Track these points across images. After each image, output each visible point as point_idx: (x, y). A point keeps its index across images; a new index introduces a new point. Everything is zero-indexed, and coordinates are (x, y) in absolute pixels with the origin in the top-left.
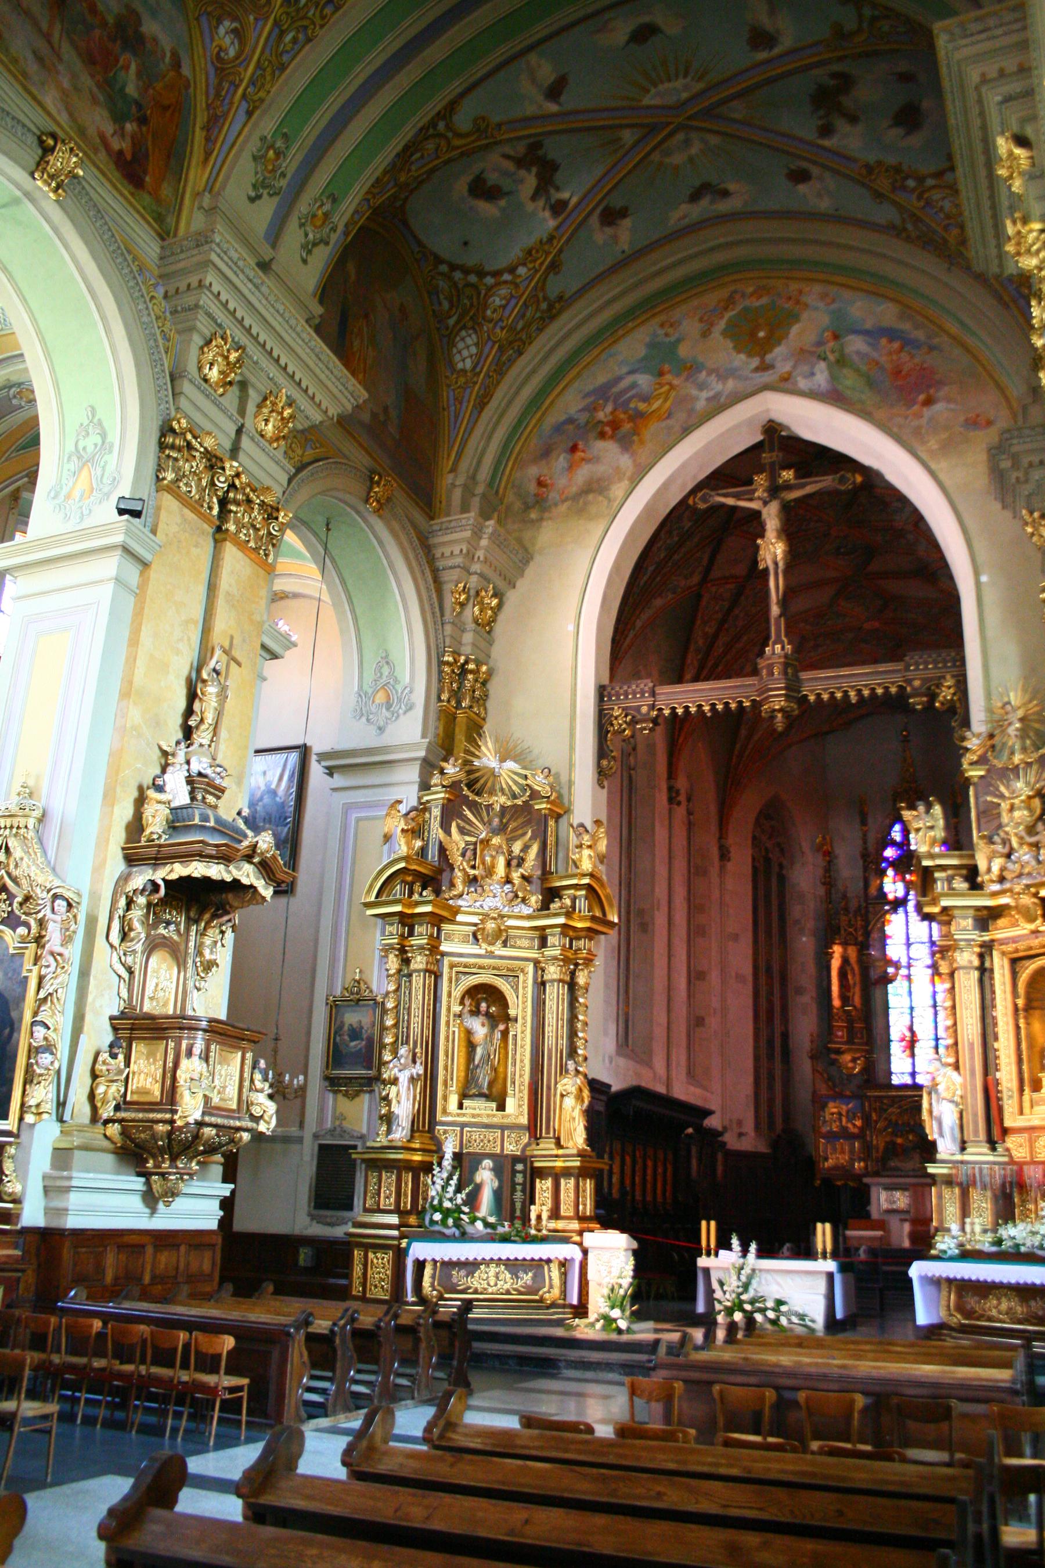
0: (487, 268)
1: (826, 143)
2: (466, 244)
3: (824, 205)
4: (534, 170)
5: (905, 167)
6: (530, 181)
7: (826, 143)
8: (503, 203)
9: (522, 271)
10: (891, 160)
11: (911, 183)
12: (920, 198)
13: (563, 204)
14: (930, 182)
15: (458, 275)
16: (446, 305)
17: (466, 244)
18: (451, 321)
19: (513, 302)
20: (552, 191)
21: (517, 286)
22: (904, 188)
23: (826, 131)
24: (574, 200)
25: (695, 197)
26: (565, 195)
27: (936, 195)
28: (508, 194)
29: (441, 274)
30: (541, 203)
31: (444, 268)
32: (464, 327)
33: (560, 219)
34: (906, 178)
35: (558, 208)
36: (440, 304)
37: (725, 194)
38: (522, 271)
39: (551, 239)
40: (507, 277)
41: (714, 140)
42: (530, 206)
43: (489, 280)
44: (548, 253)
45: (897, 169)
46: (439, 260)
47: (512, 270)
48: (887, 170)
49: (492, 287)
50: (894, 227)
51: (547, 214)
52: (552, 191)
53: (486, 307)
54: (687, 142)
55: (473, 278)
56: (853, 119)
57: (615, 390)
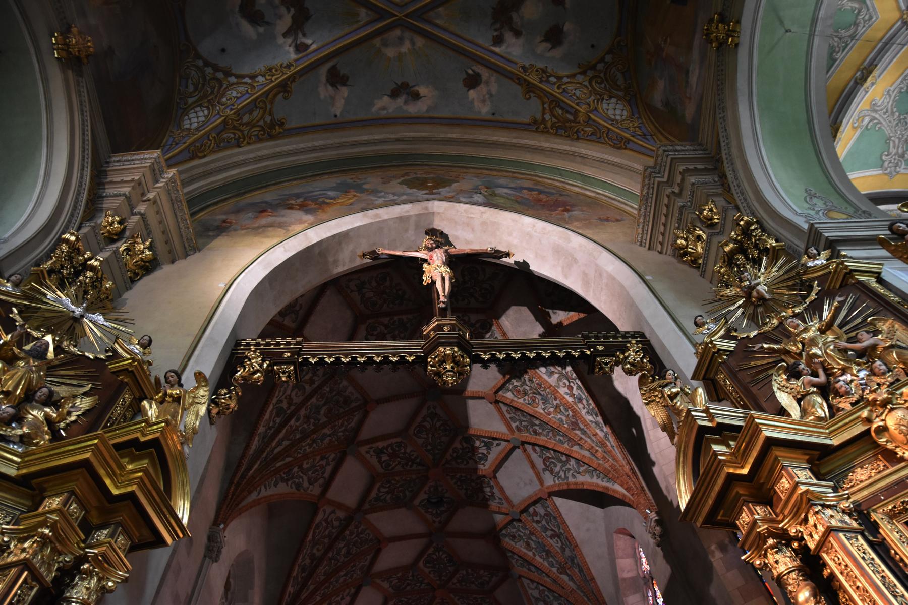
0: (233, 71)
1: (497, 50)
2: (223, 50)
3: (484, 110)
4: (292, 10)
5: (549, 70)
6: (286, 21)
7: (497, 50)
8: (261, 30)
9: (261, 79)
10: (540, 65)
11: (553, 79)
12: (559, 88)
13: (307, 47)
14: (565, 80)
15: (209, 70)
16: (191, 88)
17: (223, 50)
18: (190, 100)
19: (247, 96)
20: (300, 35)
21: (253, 87)
22: (548, 81)
23: (498, 40)
24: (314, 47)
25: (394, 94)
26: (309, 42)
27: (570, 87)
28: (268, 23)
29: (197, 67)
30: (289, 41)
31: (200, 63)
32: (201, 106)
33: (301, 55)
34: (551, 75)
35: (300, 48)
36: (187, 87)
37: (416, 96)
38: (261, 79)
39: (289, 66)
40: (247, 80)
41: (420, 42)
42: (281, 40)
43: (233, 79)
44: (284, 73)
45: (544, 71)
46: (198, 56)
47: (253, 77)
48: (537, 71)
49: (233, 84)
50: (535, 122)
51: (291, 50)
52: (300, 35)
53: (223, 95)
54: (401, 40)
55: (220, 75)
56: (517, 34)
57: (306, 195)
